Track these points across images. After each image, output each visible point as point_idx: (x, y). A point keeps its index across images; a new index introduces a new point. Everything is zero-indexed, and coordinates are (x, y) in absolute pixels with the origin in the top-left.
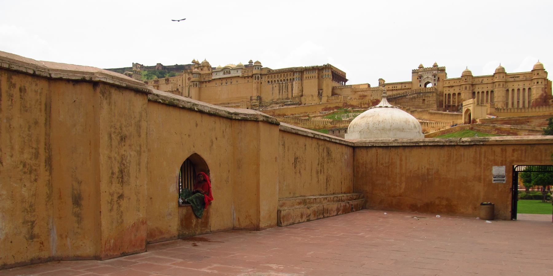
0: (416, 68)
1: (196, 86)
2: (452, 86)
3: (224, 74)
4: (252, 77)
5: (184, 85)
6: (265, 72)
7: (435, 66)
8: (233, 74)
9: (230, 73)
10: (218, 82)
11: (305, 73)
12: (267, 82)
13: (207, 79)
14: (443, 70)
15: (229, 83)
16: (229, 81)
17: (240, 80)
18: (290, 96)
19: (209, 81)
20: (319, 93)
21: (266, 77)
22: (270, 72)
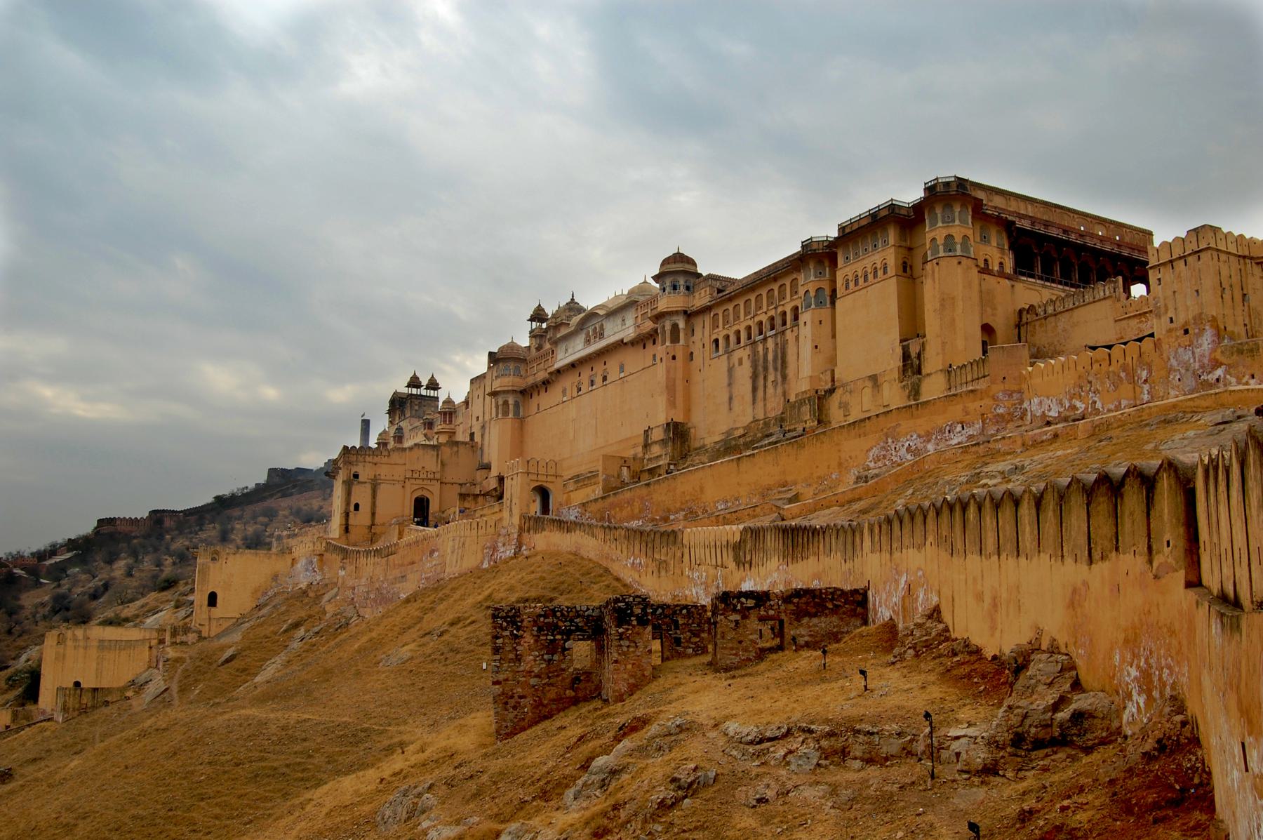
1: (506, 413)
3: (588, 342)
6: (702, 298)
9: (602, 336)
10: (569, 382)
11: (840, 261)
12: (710, 346)
13: (542, 375)
15: (598, 380)
16: (599, 369)
17: (634, 360)
19: (546, 383)
20: (906, 356)
22: (727, 292)
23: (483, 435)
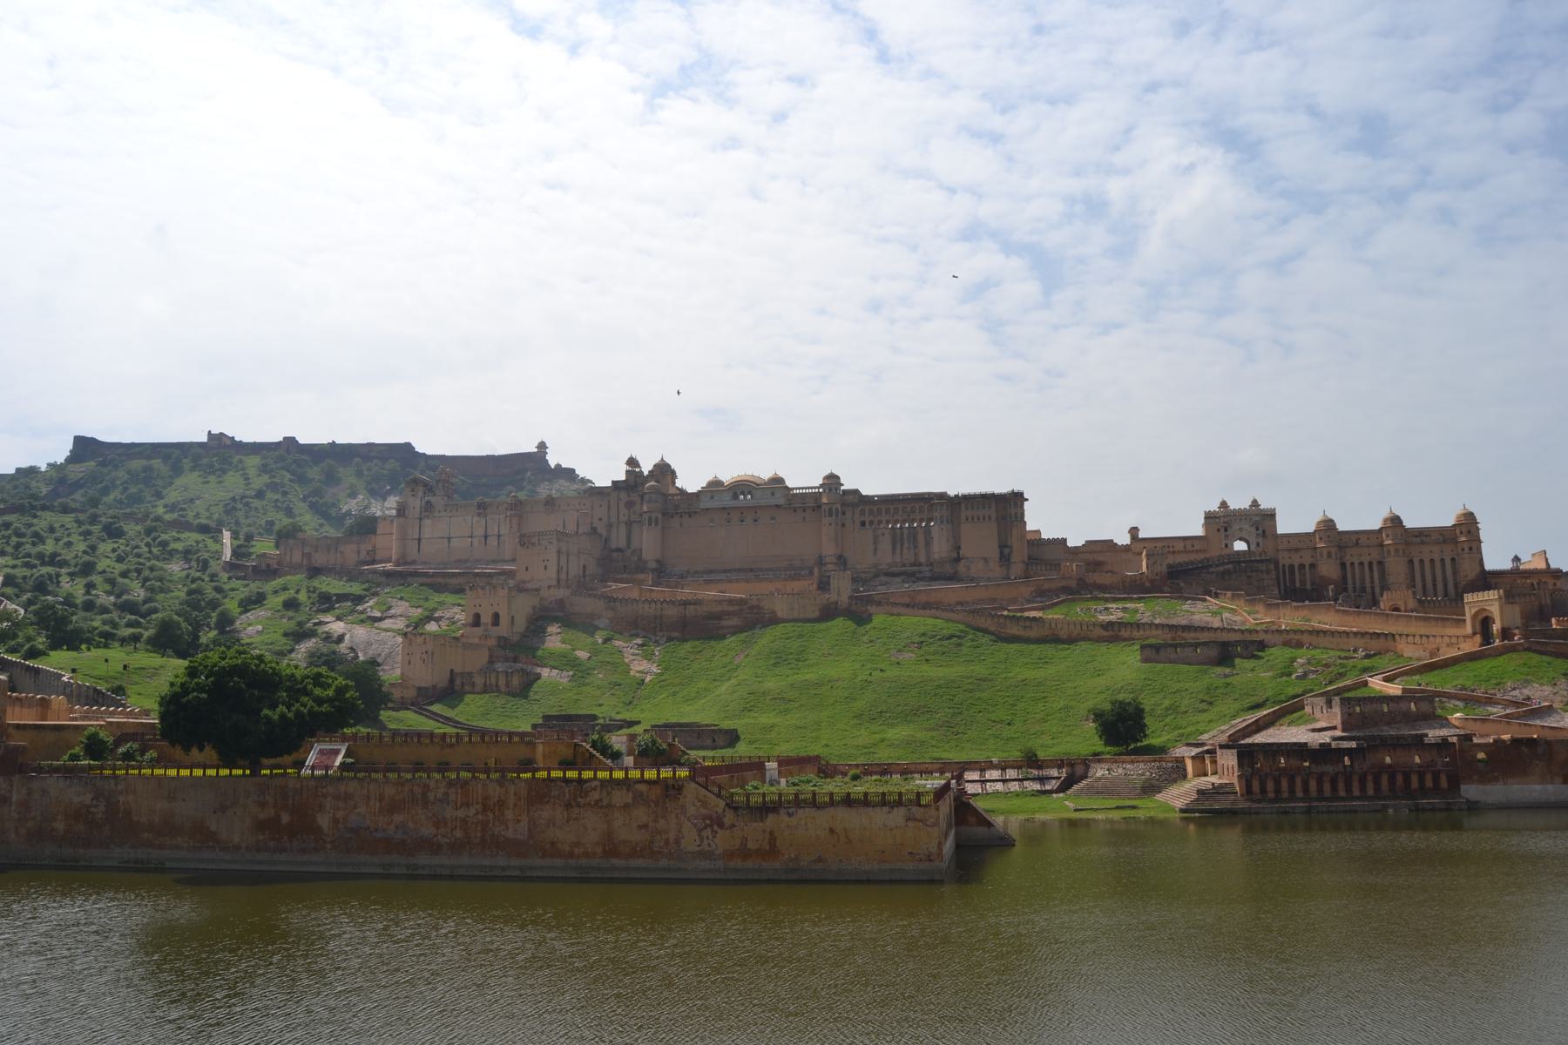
2: (1297, 550)
7: (1255, 503)
18: (922, 559)
20: (1002, 554)
23: (609, 531)
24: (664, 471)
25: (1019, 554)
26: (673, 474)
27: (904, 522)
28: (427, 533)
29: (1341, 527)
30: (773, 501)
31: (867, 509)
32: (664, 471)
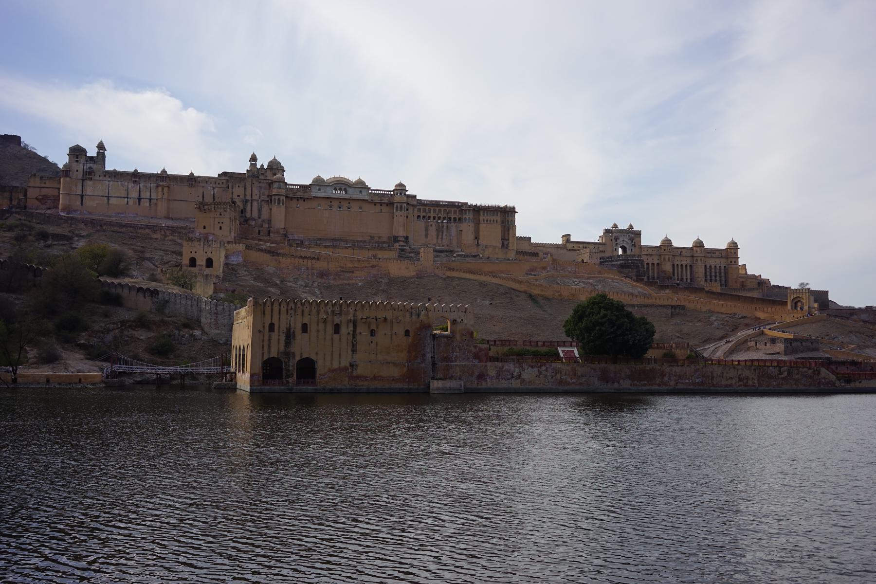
0: (610, 227)
4: (391, 204)
5: (249, 197)
7: (631, 227)
8: (353, 194)
11: (481, 212)
12: (416, 217)
14: (638, 234)
15: (345, 208)
16: (345, 205)
20: (503, 244)
21: (416, 210)
23: (245, 205)
24: (276, 167)
25: (513, 246)
26: (282, 170)
27: (444, 218)
28: (89, 191)
29: (675, 244)
30: (361, 197)
31: (422, 208)
32: (276, 167)
